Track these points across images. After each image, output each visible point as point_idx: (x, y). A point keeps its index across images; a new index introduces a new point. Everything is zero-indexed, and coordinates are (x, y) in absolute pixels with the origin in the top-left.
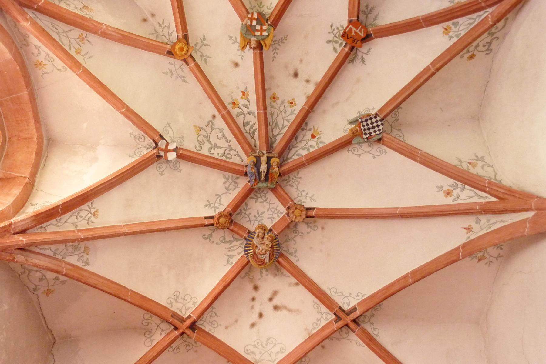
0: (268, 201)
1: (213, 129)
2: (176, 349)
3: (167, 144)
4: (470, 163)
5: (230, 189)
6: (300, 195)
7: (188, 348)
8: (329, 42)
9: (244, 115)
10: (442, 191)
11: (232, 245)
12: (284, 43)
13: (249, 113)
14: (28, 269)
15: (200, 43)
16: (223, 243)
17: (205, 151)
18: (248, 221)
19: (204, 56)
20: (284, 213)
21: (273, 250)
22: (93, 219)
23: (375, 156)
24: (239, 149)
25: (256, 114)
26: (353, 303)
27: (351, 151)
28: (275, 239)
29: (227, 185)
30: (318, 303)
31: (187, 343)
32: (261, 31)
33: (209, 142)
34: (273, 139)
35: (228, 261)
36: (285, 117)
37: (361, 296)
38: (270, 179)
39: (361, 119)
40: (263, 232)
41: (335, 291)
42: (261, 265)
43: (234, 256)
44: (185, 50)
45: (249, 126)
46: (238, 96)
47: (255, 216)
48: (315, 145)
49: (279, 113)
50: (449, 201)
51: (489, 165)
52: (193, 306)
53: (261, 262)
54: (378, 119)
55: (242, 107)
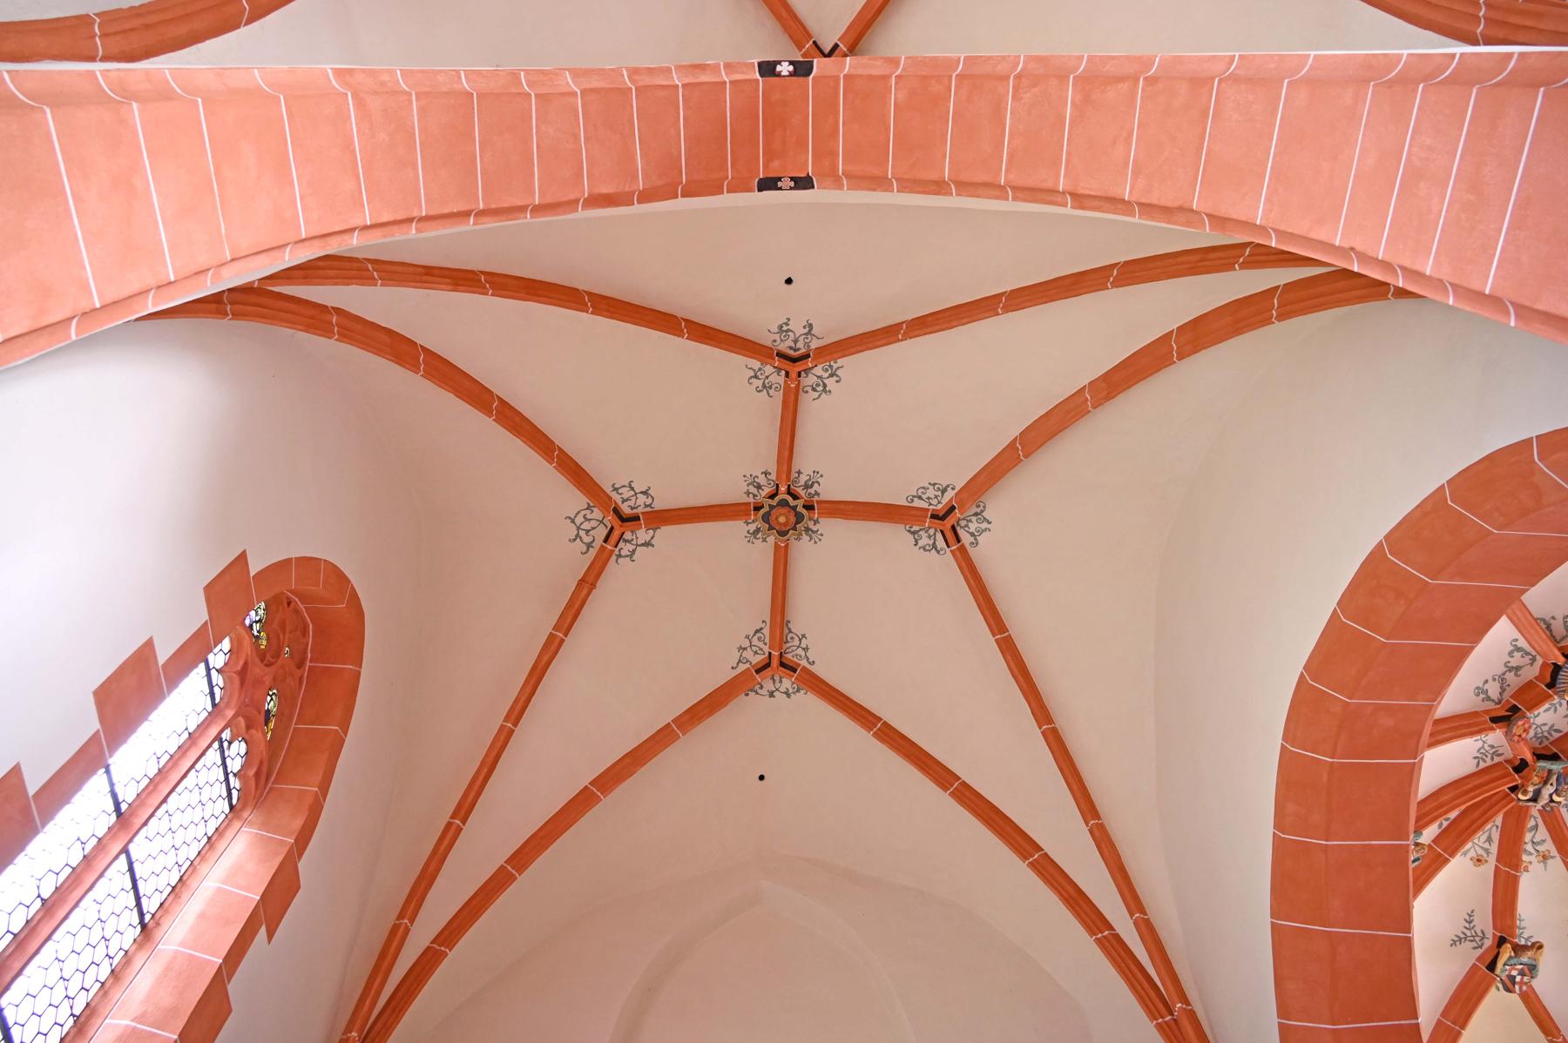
9: (1533, 842)
55: (1533, 851)
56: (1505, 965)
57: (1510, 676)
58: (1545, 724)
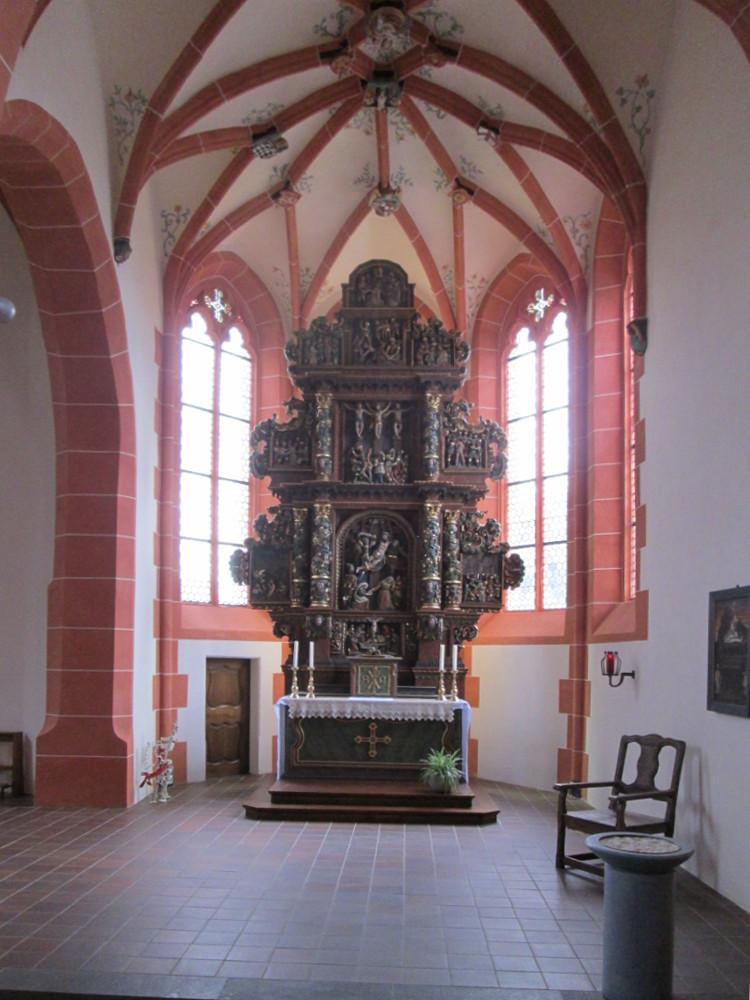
15: (443, 186)
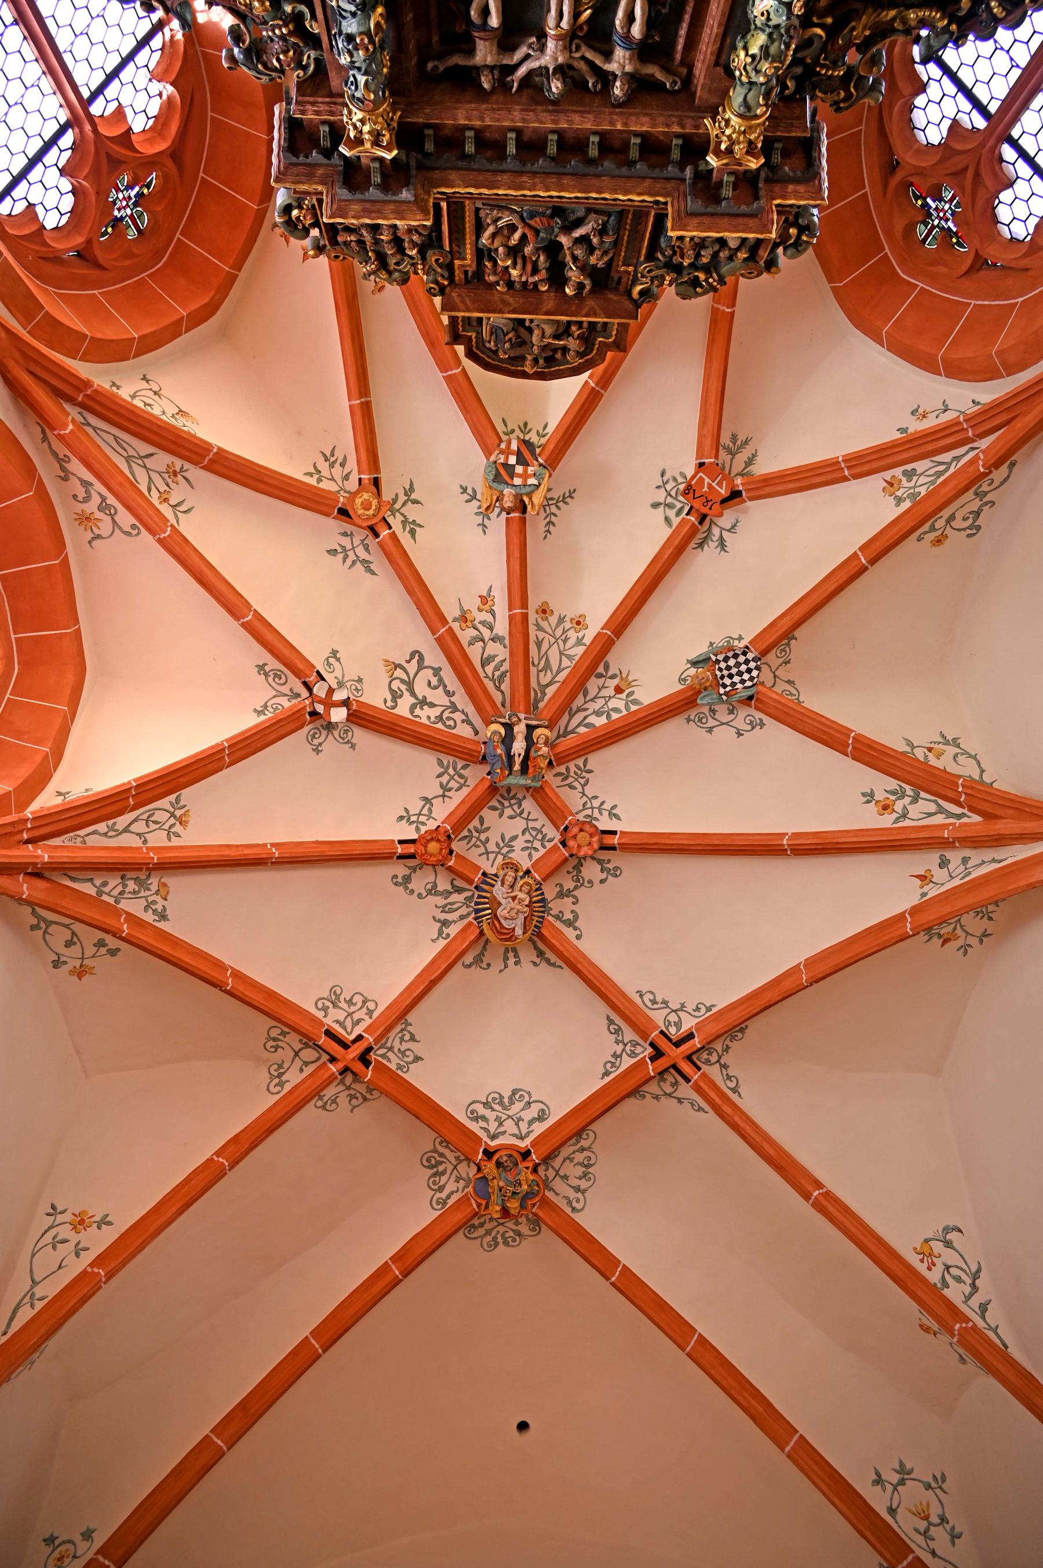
0: (525, 815)
1: (421, 667)
2: (329, 1102)
3: (331, 691)
4: (930, 750)
5: (450, 790)
6: (589, 805)
7: (354, 1102)
8: (656, 505)
9: (483, 641)
10: (874, 802)
11: (450, 900)
12: (567, 503)
13: (492, 640)
14: (44, 920)
16: (431, 894)
17: (403, 708)
18: (483, 854)
19: (409, 522)
20: (556, 841)
21: (532, 910)
22: (178, 828)
23: (742, 732)
24: (471, 710)
25: (507, 642)
26: (688, 1023)
27: (694, 721)
28: (536, 890)
29: (445, 778)
30: (617, 1022)
31: (353, 1092)
32: (525, 476)
33: (413, 694)
34: (539, 692)
35: (440, 932)
36: (564, 650)
37: (703, 1010)
38: (531, 770)
39: (716, 655)
40: (513, 874)
41: (652, 998)
42: (506, 940)
43: (451, 922)
44: (374, 508)
45: (493, 665)
46: (472, 604)
47: (497, 845)
48: (623, 709)
49: (552, 643)
50: (887, 821)
51: (968, 753)
52: (367, 1018)
53: (508, 934)
54: (750, 656)
55: (480, 627)
56: (538, 486)
57: (569, 884)
58: (511, 817)
